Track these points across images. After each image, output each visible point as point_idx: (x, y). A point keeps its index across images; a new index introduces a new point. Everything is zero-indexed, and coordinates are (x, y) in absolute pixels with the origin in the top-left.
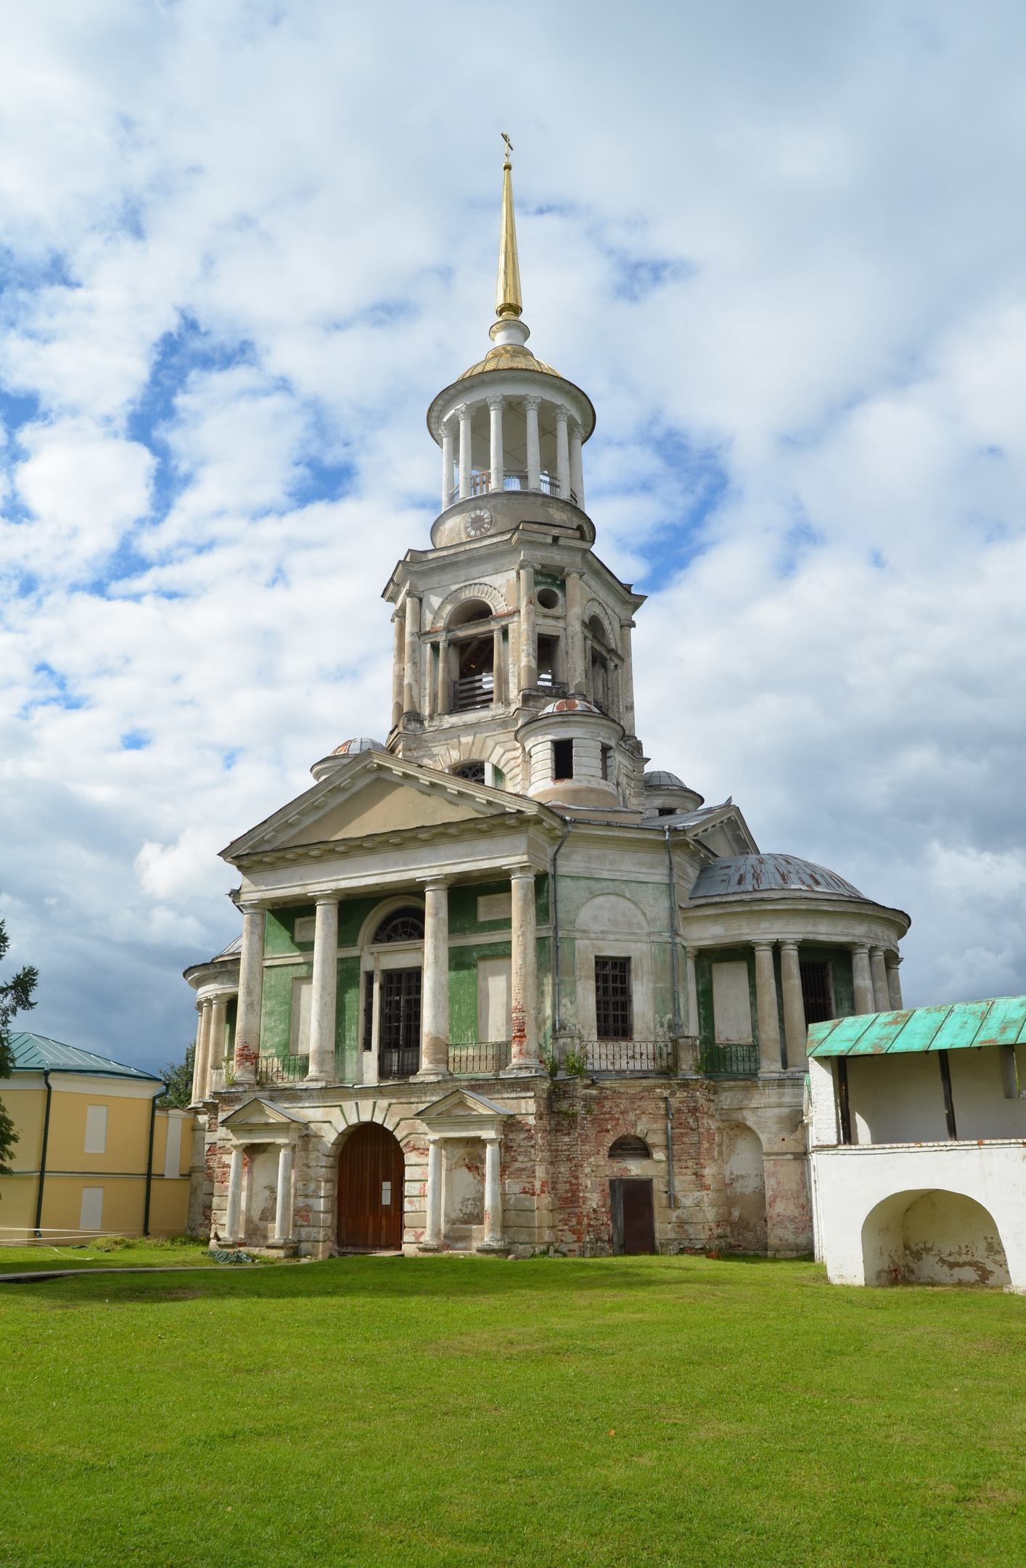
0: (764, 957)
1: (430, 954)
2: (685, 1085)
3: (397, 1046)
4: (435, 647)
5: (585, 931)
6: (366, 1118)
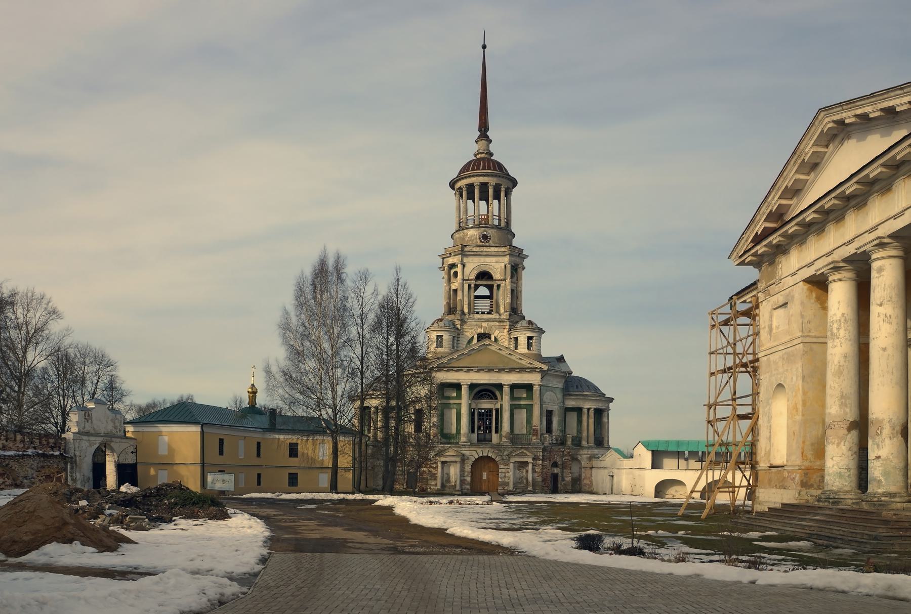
2: (569, 448)
4: (470, 286)
6: (485, 454)
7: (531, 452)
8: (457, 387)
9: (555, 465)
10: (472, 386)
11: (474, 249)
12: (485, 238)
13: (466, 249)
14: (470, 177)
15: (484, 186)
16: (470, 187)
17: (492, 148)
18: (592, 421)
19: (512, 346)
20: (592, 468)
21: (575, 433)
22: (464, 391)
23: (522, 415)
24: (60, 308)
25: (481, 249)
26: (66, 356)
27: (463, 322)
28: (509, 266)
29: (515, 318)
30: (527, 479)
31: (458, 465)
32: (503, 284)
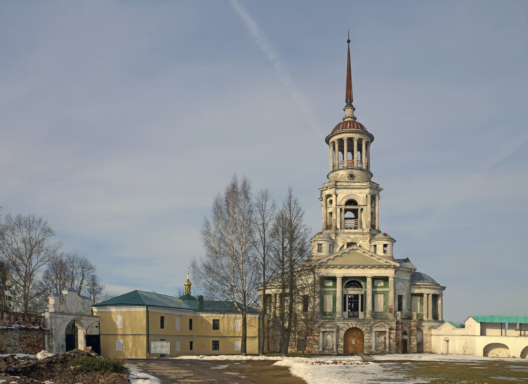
4: (341, 210)
7: (388, 324)
8: (334, 279)
9: (405, 333)
10: (344, 279)
11: (344, 184)
12: (352, 176)
13: (338, 184)
14: (340, 134)
15: (350, 140)
16: (341, 141)
17: (356, 114)
18: (430, 302)
19: (372, 250)
20: (431, 335)
23: (380, 298)
24: (53, 229)
25: (349, 184)
26: (61, 262)
27: (337, 234)
28: (369, 196)
29: (374, 232)
30: (385, 344)
31: (335, 334)
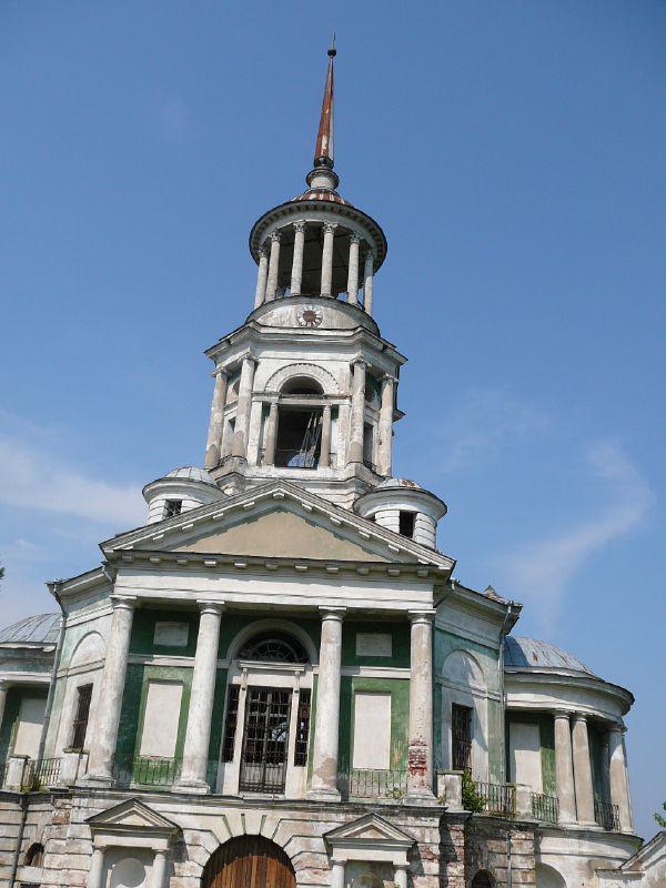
0: (561, 724)
1: (326, 674)
3: (258, 760)
4: (266, 408)
5: (448, 680)
12: (310, 316)
18: (583, 749)
21: (538, 788)
22: (209, 628)
28: (360, 373)
32: (344, 406)
